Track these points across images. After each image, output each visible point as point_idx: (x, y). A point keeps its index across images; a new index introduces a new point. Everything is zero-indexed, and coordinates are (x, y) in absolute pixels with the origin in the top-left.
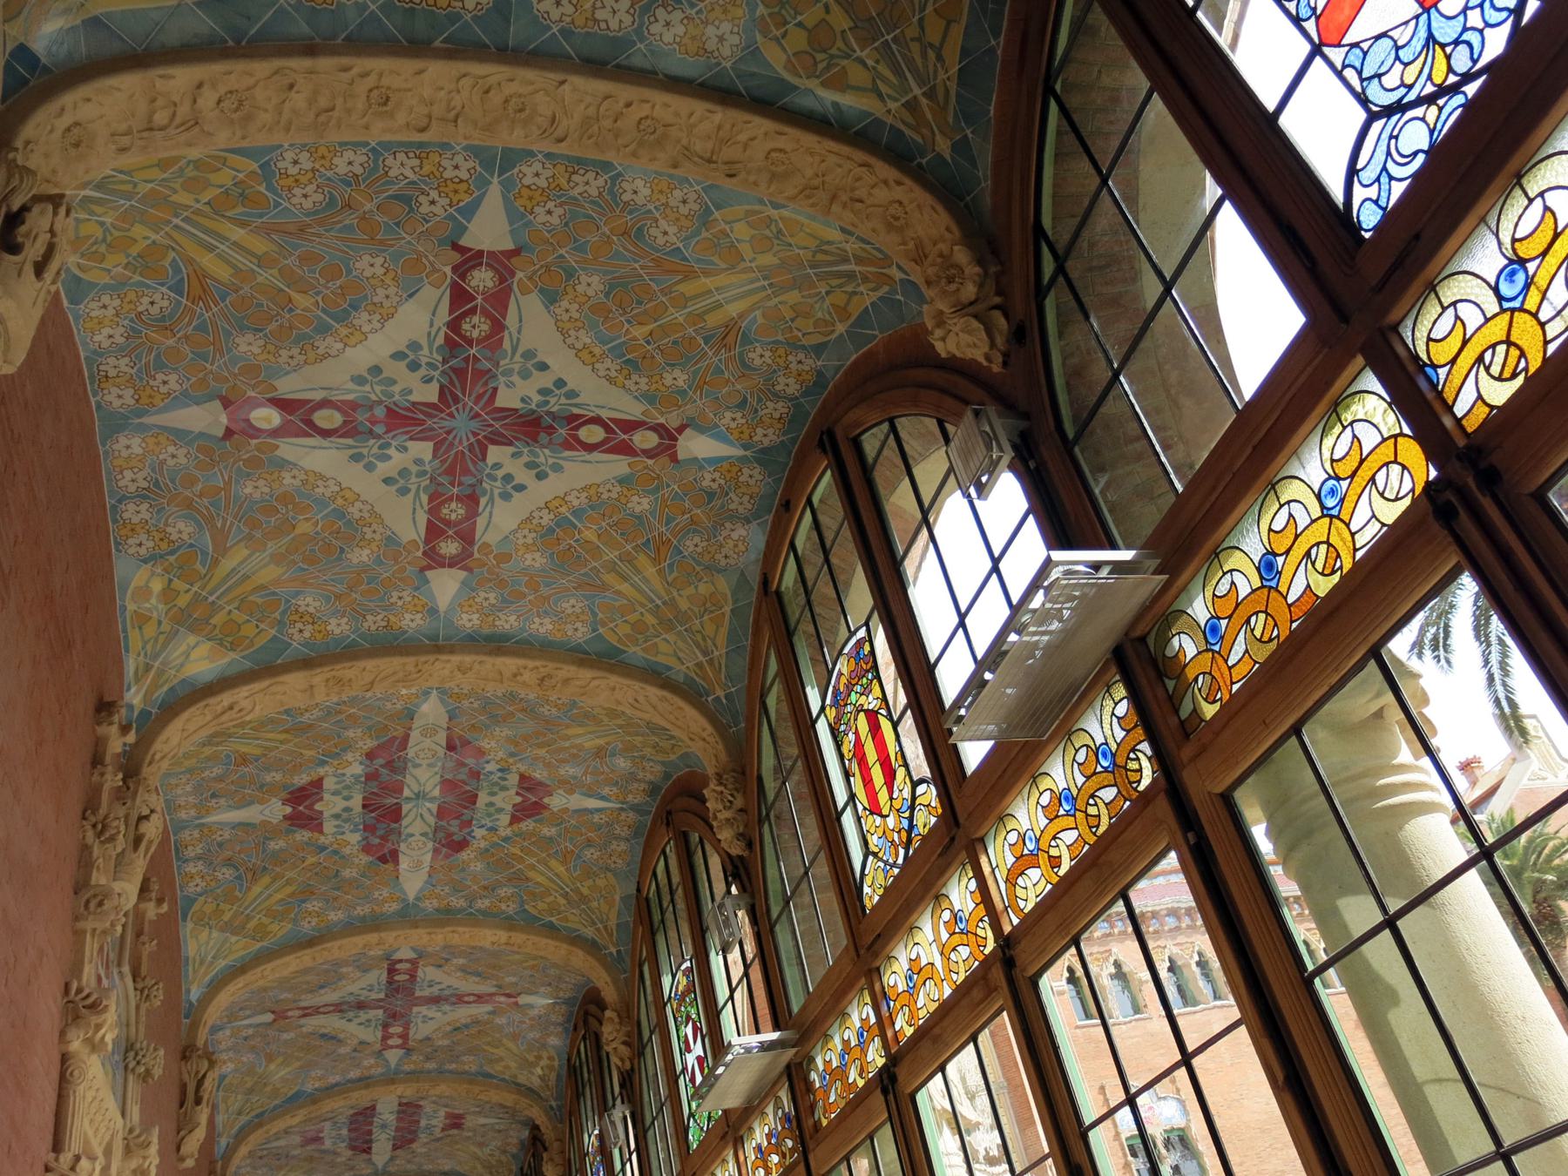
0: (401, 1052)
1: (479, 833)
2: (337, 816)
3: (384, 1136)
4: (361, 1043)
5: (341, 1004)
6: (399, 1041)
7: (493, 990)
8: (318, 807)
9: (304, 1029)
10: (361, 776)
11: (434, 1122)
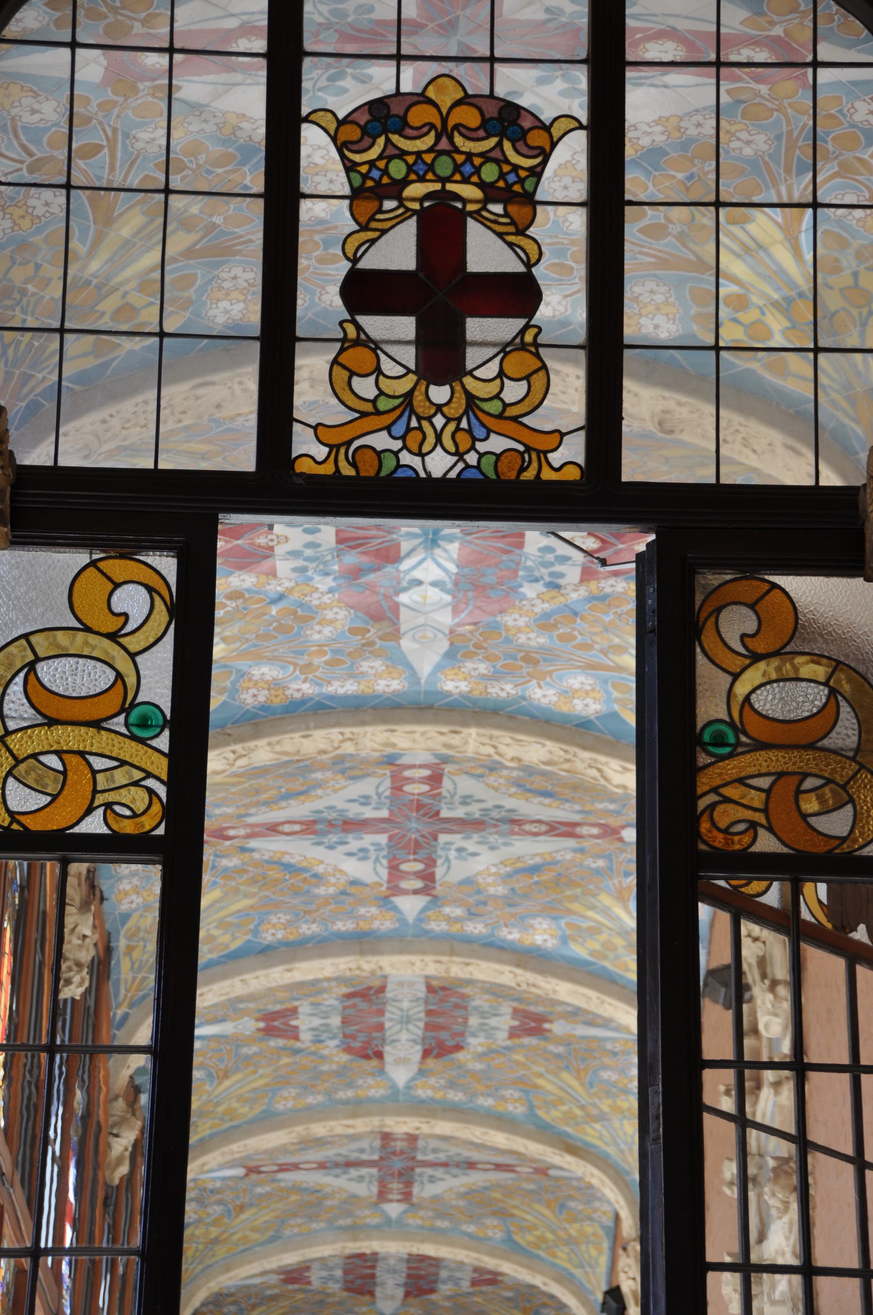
0: (420, 901)
1: (529, 591)
3: (404, 1036)
4: (354, 883)
5: (315, 822)
6: (419, 884)
7: (577, 818)
9: (256, 856)
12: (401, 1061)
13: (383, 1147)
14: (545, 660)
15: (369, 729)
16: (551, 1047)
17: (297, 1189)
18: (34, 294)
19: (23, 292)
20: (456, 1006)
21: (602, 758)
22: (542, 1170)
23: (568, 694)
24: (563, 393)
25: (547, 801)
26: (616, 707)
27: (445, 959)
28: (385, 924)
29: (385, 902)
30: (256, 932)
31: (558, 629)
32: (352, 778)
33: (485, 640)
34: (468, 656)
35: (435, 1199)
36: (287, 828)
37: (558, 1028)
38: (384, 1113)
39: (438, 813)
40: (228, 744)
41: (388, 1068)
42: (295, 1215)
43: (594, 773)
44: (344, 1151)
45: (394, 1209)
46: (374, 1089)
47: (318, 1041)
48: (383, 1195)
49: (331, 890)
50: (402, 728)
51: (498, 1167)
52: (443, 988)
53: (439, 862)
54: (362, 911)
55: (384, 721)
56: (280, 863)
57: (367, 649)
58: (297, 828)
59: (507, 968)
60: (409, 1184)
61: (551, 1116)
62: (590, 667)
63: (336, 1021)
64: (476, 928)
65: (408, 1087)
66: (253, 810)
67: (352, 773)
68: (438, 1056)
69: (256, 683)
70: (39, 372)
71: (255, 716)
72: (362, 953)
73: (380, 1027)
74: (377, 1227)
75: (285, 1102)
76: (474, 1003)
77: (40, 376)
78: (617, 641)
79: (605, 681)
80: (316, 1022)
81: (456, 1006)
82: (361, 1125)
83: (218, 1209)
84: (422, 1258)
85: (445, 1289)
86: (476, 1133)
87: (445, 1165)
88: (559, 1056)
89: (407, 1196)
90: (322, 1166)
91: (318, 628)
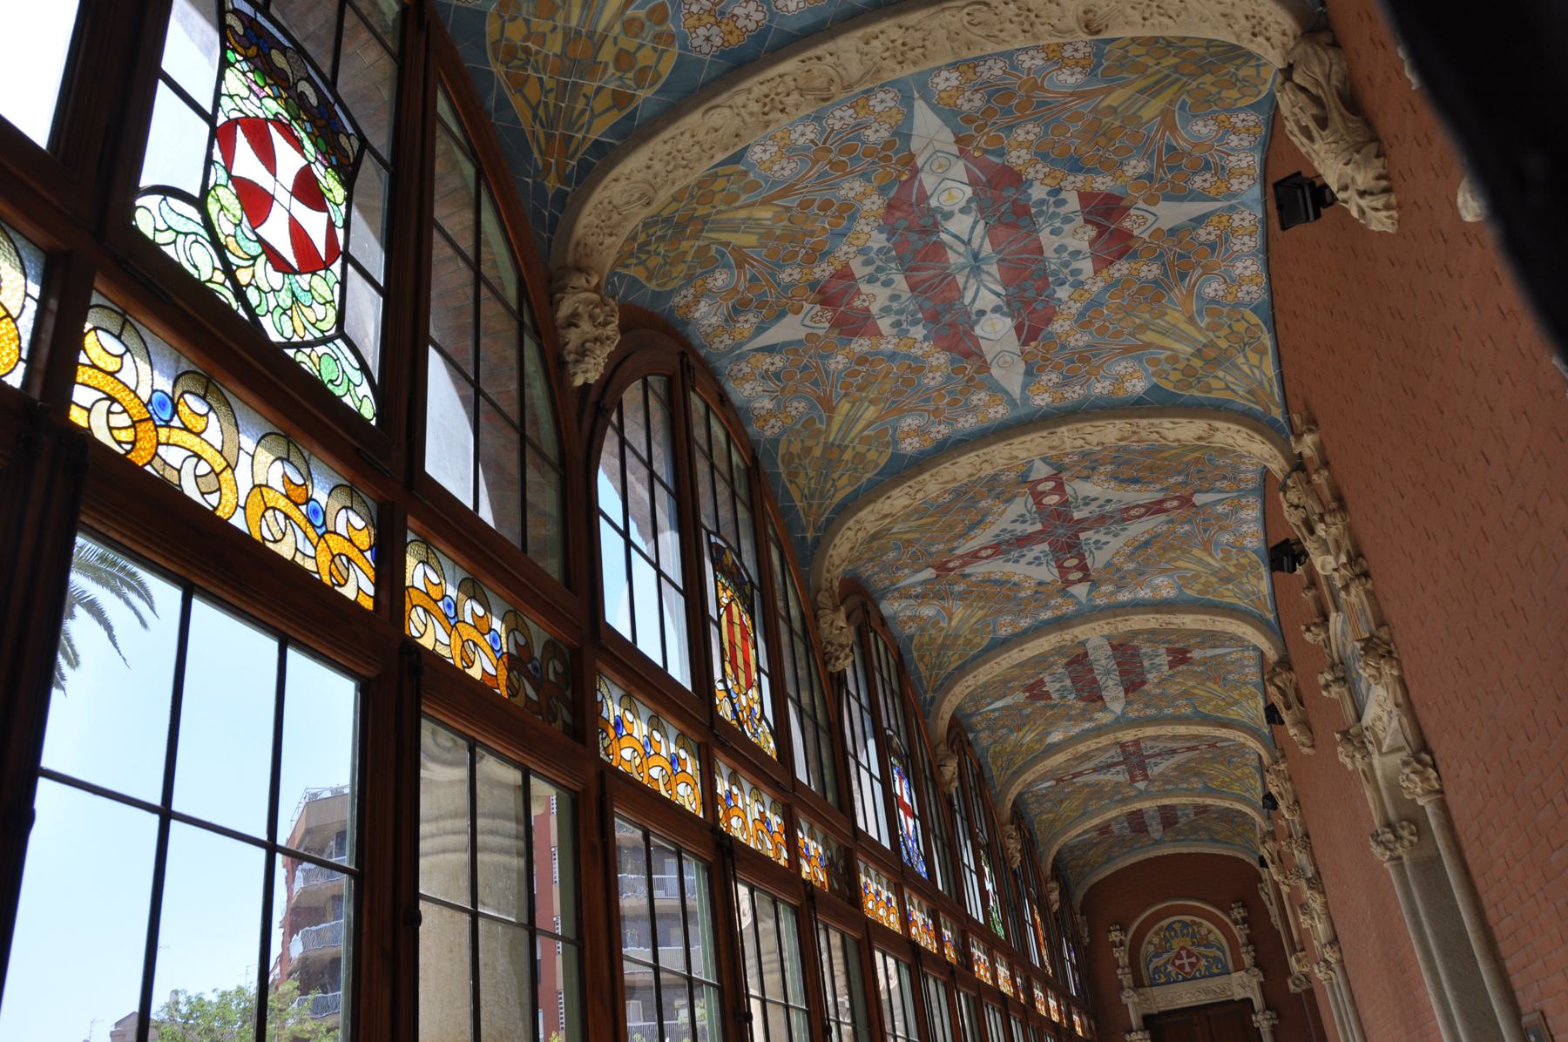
2: (886, 310)
3: (1110, 683)
4: (1040, 584)
5: (998, 544)
6: (1079, 575)
7: (1160, 496)
8: (857, 303)
10: (889, 250)
11: (1157, 661)
12: (1115, 699)
13: (1123, 752)
14: (1095, 356)
15: (994, 447)
16: (1195, 668)
17: (1086, 785)
18: (538, 53)
19: (527, 51)
20: (1133, 656)
21: (1156, 421)
22: (1213, 744)
23: (1119, 380)
24: (1001, 31)
25: (1137, 487)
26: (1155, 380)
27: (1112, 620)
28: (1070, 609)
29: (1063, 592)
30: (994, 631)
31: (1093, 324)
32: (1007, 501)
33: (1048, 351)
34: (1041, 369)
35: (1161, 774)
36: (984, 553)
37: (1196, 654)
38: (1115, 731)
39: (1072, 519)
40: (904, 482)
41: (1108, 705)
42: (1090, 799)
43: (1155, 436)
44: (1102, 759)
45: (1141, 785)
46: (1103, 718)
47: (1063, 697)
48: (1133, 780)
49: (1029, 592)
50: (1017, 441)
51: (1189, 749)
52: (1121, 645)
53: (1087, 554)
54: (1053, 602)
55: (1003, 439)
56: (989, 581)
57: (971, 385)
58: (989, 552)
59: (1150, 616)
60: (1144, 769)
61: (1207, 709)
62: (1127, 351)
63: (1068, 682)
64: (1124, 596)
65: (1124, 714)
66: (956, 544)
67: (1005, 497)
68: (1133, 691)
69: (908, 433)
70: (577, 132)
71: (918, 459)
72: (1062, 629)
73: (1094, 681)
74: (1135, 796)
75: (1056, 737)
76: (1143, 651)
77: (580, 136)
78: (1138, 321)
79: (1141, 361)
80: (1058, 686)
81: (1133, 656)
82: (1104, 740)
83: (1049, 804)
84: (1165, 807)
85: (1183, 820)
86: (1168, 730)
87: (1159, 754)
88: (1202, 673)
89: (1146, 777)
90: (1095, 770)
91: (931, 375)
